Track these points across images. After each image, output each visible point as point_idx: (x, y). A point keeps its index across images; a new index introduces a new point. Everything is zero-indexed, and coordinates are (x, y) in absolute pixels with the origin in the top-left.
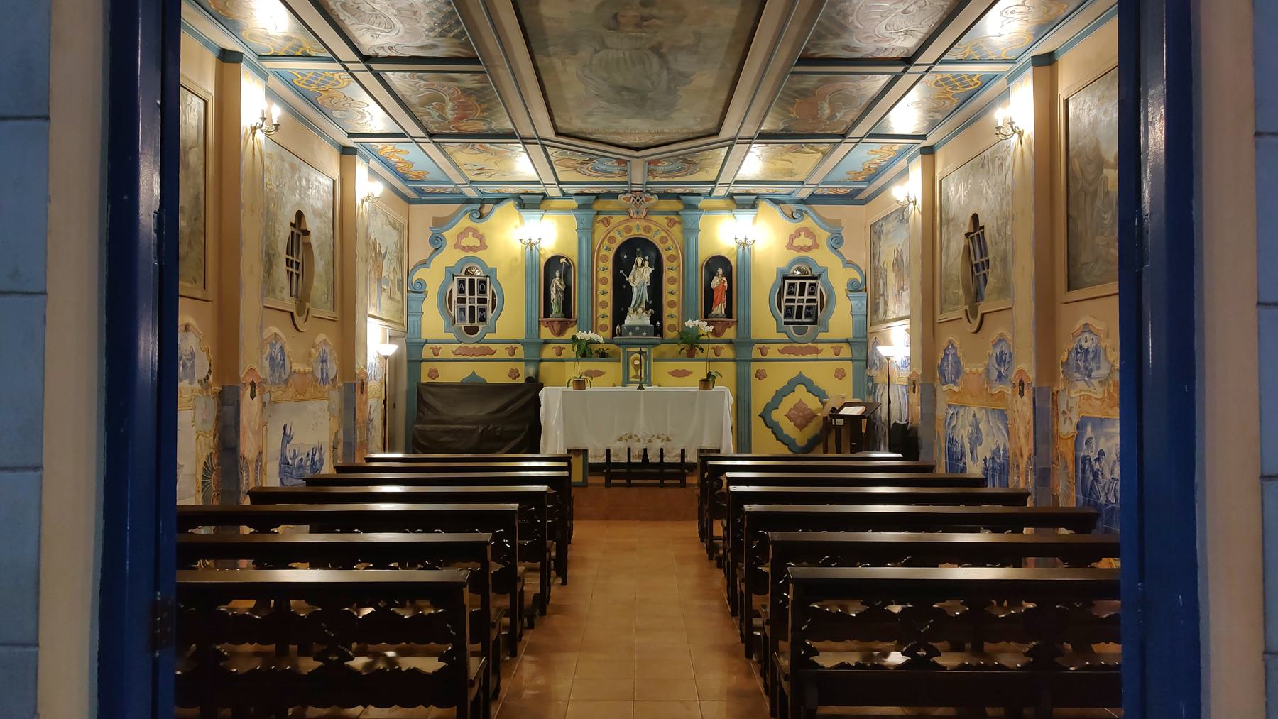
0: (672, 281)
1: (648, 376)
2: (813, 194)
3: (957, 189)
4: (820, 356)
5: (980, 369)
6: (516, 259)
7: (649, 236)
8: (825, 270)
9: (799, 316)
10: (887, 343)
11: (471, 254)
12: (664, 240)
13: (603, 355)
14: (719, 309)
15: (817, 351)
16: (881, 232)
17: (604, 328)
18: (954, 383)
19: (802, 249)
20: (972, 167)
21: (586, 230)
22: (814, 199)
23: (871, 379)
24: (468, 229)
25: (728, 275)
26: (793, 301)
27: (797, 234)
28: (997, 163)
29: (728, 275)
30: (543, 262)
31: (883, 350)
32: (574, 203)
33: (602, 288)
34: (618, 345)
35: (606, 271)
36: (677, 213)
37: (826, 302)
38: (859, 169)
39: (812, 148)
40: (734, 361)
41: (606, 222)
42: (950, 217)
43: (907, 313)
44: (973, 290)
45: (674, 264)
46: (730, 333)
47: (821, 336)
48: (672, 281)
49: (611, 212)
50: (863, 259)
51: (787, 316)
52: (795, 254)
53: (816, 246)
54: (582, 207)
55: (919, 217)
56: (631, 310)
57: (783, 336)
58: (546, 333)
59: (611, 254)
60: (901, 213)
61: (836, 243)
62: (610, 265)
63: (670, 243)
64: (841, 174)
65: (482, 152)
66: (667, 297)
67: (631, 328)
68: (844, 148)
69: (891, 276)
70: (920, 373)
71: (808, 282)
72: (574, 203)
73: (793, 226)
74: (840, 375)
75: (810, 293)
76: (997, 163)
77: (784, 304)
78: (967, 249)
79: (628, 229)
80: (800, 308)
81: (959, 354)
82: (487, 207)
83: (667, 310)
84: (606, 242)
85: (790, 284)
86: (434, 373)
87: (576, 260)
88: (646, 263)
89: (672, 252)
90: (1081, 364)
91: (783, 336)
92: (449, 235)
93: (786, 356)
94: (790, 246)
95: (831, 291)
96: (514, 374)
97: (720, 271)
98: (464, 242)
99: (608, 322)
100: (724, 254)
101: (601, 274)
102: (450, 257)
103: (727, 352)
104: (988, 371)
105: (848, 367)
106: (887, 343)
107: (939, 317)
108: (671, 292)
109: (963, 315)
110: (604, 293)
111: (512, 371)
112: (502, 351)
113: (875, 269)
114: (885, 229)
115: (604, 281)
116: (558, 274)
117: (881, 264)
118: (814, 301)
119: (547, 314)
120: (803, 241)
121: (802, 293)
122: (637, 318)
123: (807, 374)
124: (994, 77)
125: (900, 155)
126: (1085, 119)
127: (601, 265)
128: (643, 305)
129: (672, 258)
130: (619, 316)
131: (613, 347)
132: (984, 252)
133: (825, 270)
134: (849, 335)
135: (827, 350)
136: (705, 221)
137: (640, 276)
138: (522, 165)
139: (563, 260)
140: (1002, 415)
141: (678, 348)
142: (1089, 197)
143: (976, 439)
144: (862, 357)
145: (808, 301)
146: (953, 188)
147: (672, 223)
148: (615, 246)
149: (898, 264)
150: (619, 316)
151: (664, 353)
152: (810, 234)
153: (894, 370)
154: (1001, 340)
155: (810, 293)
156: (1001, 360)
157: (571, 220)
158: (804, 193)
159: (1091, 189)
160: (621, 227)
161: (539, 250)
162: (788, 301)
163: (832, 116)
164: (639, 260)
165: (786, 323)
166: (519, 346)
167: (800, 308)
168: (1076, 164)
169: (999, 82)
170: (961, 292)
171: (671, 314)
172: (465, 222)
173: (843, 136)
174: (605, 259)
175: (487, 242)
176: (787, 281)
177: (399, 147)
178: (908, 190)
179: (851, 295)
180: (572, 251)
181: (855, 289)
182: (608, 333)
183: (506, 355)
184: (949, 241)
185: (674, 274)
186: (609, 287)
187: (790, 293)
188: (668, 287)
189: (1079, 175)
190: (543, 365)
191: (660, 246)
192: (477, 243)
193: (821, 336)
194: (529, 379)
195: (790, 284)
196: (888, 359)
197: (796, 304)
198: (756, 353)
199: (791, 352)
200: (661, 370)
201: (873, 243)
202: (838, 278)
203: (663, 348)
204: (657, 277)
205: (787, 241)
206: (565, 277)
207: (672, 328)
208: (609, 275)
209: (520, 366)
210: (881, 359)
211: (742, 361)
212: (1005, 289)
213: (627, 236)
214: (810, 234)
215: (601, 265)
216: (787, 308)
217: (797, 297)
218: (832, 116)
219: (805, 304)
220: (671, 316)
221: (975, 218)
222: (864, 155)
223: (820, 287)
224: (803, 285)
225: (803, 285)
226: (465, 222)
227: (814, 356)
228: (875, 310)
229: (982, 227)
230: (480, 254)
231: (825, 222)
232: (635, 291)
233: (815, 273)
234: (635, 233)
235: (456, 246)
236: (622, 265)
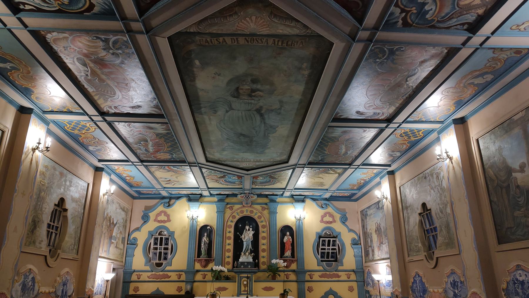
0: (264, 238)
1: (251, 291)
2: (331, 196)
3: (410, 191)
4: (340, 279)
5: (440, 290)
6: (185, 227)
7: (252, 215)
8: (340, 233)
9: (328, 257)
10: (376, 272)
11: (162, 224)
12: (260, 217)
13: (227, 279)
14: (288, 253)
16: (366, 215)
17: (228, 263)
19: (328, 222)
20: (419, 179)
21: (221, 212)
22: (333, 198)
23: (368, 292)
24: (161, 212)
25: (292, 235)
26: (325, 249)
28: (435, 176)
29: (292, 235)
30: (198, 228)
31: (376, 277)
32: (215, 199)
33: (228, 242)
34: (235, 272)
35: (230, 233)
36: (266, 204)
37: (342, 250)
38: (355, 183)
39: (334, 171)
40: (296, 281)
41: (231, 208)
42: (408, 205)
43: (388, 256)
44: (427, 244)
45: (265, 230)
46: (294, 266)
47: (340, 268)
48: (264, 238)
49: (234, 204)
50: (358, 228)
51: (322, 257)
52: (324, 225)
53: (334, 221)
54: (220, 201)
55: (390, 206)
56: (242, 254)
57: (321, 268)
58: (198, 266)
59: (233, 224)
60: (378, 205)
61: (344, 220)
62: (232, 230)
63: (262, 219)
64: (346, 186)
65: (169, 171)
66: (261, 247)
67: (243, 263)
68: (350, 171)
69: (375, 237)
70: (400, 290)
71: (331, 239)
72: (215, 199)
73: (323, 211)
74: (351, 289)
75: (333, 245)
76: (435, 176)
77: (320, 251)
78: (421, 222)
79: (242, 212)
80: (328, 253)
82: (173, 201)
83: (262, 254)
84: (231, 218)
85: (323, 241)
86: (136, 289)
87: (215, 227)
88: (251, 229)
89: (264, 223)
90: (520, 291)
91: (321, 268)
92: (152, 215)
94: (322, 221)
95: (343, 244)
96: (180, 289)
97: (288, 233)
98: (159, 218)
99: (230, 260)
100: (290, 225)
101: (228, 235)
102: (152, 226)
103: (293, 277)
104: (445, 291)
105: (355, 285)
106: (376, 272)
107: (407, 259)
108: (263, 244)
109: (424, 258)
110: (229, 244)
111: (178, 287)
112: (174, 276)
113: (365, 234)
114: (369, 213)
115: (229, 238)
116: (206, 234)
117: (368, 230)
118: (335, 249)
119: (199, 256)
120: (328, 219)
121: (329, 245)
122: (246, 258)
124: (432, 131)
125: (376, 175)
126: (493, 148)
127: (228, 230)
128: (249, 251)
129: (264, 227)
130: (236, 256)
131: (233, 274)
132: (431, 222)
133: (340, 233)
134: (354, 267)
136: (280, 208)
137: (248, 235)
138: (191, 179)
139: (208, 227)
141: (267, 274)
142: (504, 190)
144: (362, 279)
145: (332, 249)
146: (408, 191)
147: (264, 209)
148: (235, 220)
149: (378, 230)
150: (236, 256)
151: (260, 277)
152: (331, 215)
153: (382, 288)
154: (453, 273)
155: (333, 245)
156: (454, 284)
157: (214, 207)
158: (327, 195)
159: (505, 185)
160: (239, 211)
161: (197, 222)
162: (322, 249)
163: (346, 153)
164: (247, 227)
165: (322, 261)
166: (183, 273)
167: (328, 253)
168: (491, 172)
169: (433, 135)
170: (420, 245)
171: (263, 256)
172: (161, 208)
173: (350, 164)
174: (230, 227)
175: (171, 218)
176: (321, 239)
177: (127, 168)
178: (383, 191)
179: (353, 246)
180: (214, 223)
181: (355, 243)
182: (230, 267)
183: (177, 279)
184: (409, 218)
185: (264, 235)
186: (231, 241)
187: (323, 245)
188: (262, 241)
189: (494, 177)
190: (195, 284)
191: (258, 220)
192: (166, 218)
193: (340, 268)
194: (187, 292)
195: (323, 241)
196: (378, 281)
197: (326, 251)
198: (307, 278)
199: (326, 277)
200: (258, 287)
201: (362, 220)
202: (347, 238)
203: (260, 274)
204: (256, 236)
205: (320, 219)
206: (209, 236)
207: (264, 263)
208: (232, 235)
209: (183, 285)
210: (373, 280)
211: (300, 282)
212: (452, 242)
213: (241, 215)
214: (331, 215)
215: (228, 230)
216: (322, 253)
217: (327, 247)
218: (346, 153)
219: (331, 251)
220: (263, 257)
221: (424, 205)
222: (359, 175)
223: (338, 242)
224: (329, 241)
225: (329, 241)
226: (161, 208)
228: (367, 254)
229: (430, 210)
230: (166, 225)
231: (338, 210)
232: (245, 243)
233: (335, 235)
234: (245, 214)
235: (155, 220)
236: (239, 230)
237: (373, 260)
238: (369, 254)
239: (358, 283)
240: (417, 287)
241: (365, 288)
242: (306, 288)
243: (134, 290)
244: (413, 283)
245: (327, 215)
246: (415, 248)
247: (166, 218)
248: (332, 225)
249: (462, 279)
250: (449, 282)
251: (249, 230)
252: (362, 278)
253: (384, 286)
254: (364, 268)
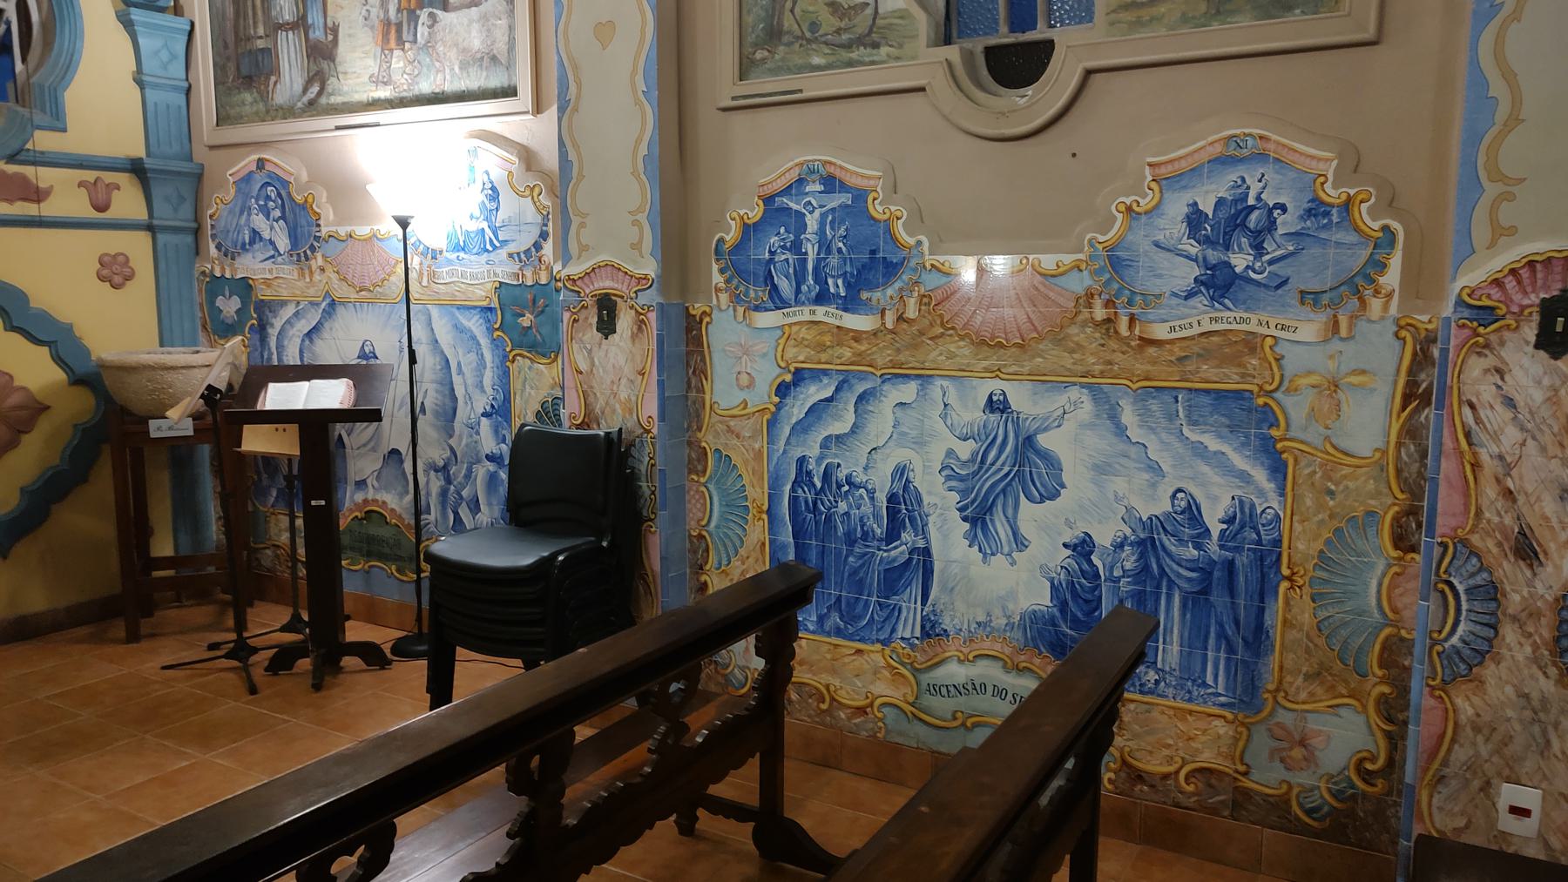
4: (48, 209)
15: (38, 195)
18: (850, 303)
23: (244, 287)
47: (44, 141)
81: (877, 210)
105: (138, 247)
109: (939, 82)
134: (139, 151)
135: (66, 195)
140: (1250, 415)
143: (1009, 473)
227: (31, 209)
228: (245, 69)
237: (313, 108)
238: (275, 70)
239: (161, 238)
240: (796, 247)
241: (212, 261)
244: (750, 231)
246: (829, 22)
249: (1332, 194)
250: (1177, 207)
252: (186, 211)
253: (435, 255)
254: (200, 154)
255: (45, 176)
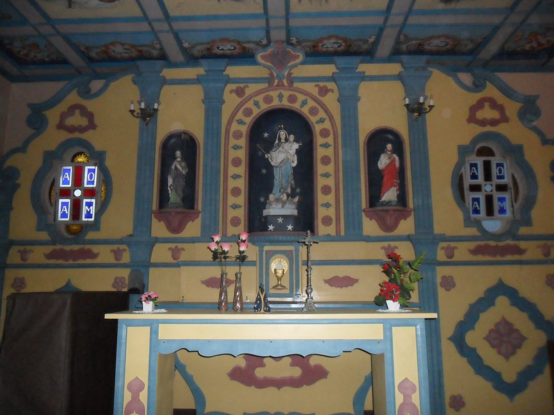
4: (524, 257)
11: (77, 135)
12: (313, 111)
15: (521, 252)
24: (72, 109)
27: (479, 105)
52: (478, 130)
53: (504, 119)
57: (473, 231)
86: (20, 283)
88: (292, 138)
92: (53, 116)
93: (479, 258)
94: (472, 119)
97: (389, 146)
98: (71, 121)
120: (487, 113)
123: (510, 281)
129: (325, 133)
137: (284, 154)
152: (494, 105)
164: (283, 134)
172: (73, 98)
175: (97, 121)
183: (111, 259)
192: (84, 122)
204: (306, 155)
208: (242, 154)
214: (494, 105)
226: (73, 98)
227: (516, 257)
230: (87, 136)
234: (276, 103)
235: (61, 126)
242: (439, 280)
243: (13, 286)
245: (487, 104)
247: (84, 122)
248: (502, 129)
251: (287, 140)
255: (523, 244)
